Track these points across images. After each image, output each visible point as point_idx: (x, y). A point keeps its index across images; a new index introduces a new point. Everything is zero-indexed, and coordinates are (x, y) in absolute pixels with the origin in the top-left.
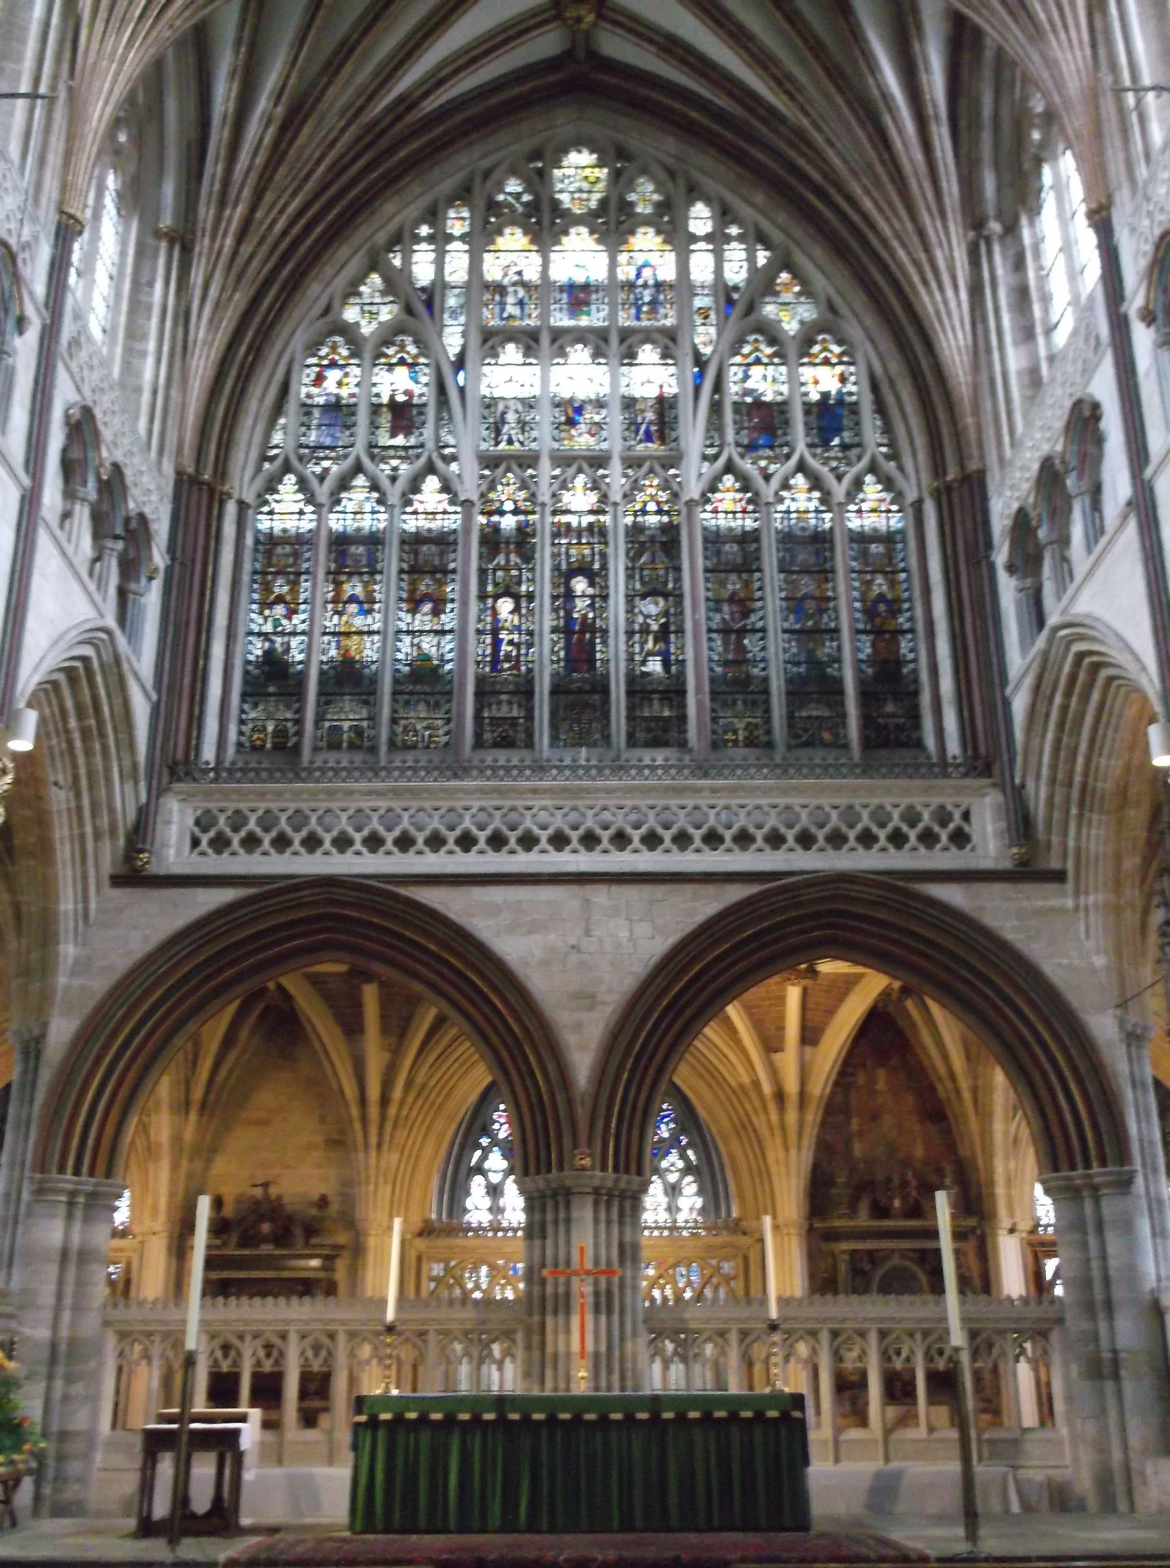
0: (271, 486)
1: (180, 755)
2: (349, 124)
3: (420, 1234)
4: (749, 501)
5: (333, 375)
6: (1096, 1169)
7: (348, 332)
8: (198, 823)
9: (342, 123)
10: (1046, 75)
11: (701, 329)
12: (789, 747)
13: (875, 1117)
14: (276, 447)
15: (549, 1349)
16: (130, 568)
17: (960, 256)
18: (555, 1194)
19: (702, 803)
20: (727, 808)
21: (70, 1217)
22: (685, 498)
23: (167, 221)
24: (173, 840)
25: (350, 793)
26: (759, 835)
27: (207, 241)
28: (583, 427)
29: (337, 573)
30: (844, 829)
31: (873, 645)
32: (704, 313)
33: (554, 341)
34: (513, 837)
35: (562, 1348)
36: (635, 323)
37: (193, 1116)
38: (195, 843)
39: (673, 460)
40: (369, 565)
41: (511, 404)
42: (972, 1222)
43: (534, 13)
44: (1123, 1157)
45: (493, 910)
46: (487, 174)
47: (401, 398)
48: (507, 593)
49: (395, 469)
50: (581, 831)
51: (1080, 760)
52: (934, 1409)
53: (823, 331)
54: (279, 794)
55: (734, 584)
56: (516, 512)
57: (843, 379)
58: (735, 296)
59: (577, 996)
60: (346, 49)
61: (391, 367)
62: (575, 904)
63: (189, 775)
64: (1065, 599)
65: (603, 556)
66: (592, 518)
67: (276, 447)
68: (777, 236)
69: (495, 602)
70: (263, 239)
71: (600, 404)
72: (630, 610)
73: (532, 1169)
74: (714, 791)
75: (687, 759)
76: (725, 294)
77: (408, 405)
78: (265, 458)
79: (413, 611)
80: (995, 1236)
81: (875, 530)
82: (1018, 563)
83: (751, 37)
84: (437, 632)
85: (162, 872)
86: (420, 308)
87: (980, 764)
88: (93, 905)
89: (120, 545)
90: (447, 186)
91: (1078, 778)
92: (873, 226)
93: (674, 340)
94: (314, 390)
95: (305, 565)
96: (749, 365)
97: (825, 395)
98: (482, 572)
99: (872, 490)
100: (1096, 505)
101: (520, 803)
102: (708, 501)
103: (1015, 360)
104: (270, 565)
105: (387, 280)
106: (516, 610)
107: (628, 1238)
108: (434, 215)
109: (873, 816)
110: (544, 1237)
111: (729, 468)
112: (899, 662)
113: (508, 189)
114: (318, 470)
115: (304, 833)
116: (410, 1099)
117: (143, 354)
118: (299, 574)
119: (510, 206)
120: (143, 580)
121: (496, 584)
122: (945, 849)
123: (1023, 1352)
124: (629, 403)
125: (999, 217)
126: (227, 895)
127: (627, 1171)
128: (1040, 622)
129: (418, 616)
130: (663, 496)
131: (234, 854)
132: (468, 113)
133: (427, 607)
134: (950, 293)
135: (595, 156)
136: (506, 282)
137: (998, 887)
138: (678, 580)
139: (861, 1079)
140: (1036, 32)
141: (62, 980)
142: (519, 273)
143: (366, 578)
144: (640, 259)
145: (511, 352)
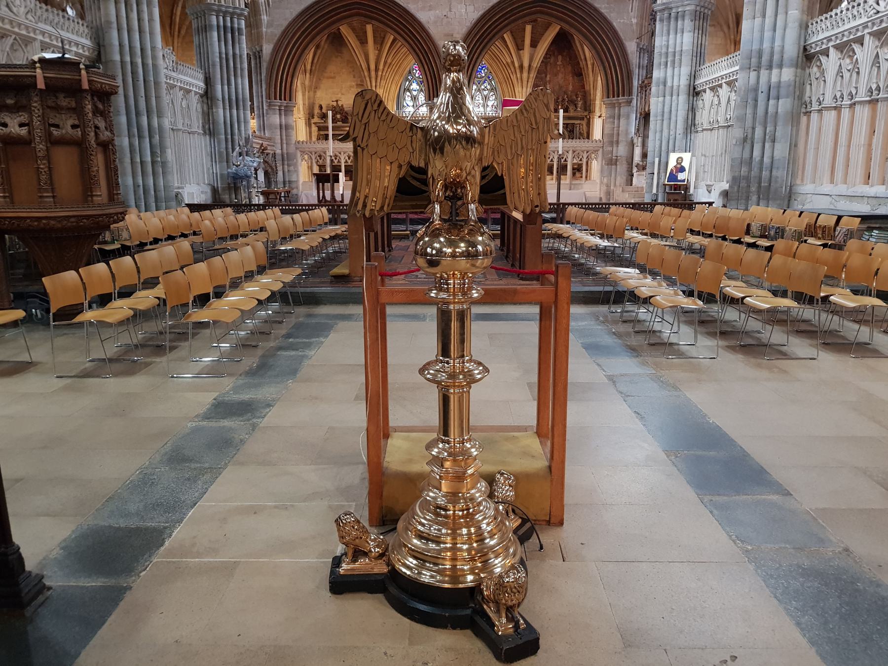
80: (593, 118)
116: (386, 69)
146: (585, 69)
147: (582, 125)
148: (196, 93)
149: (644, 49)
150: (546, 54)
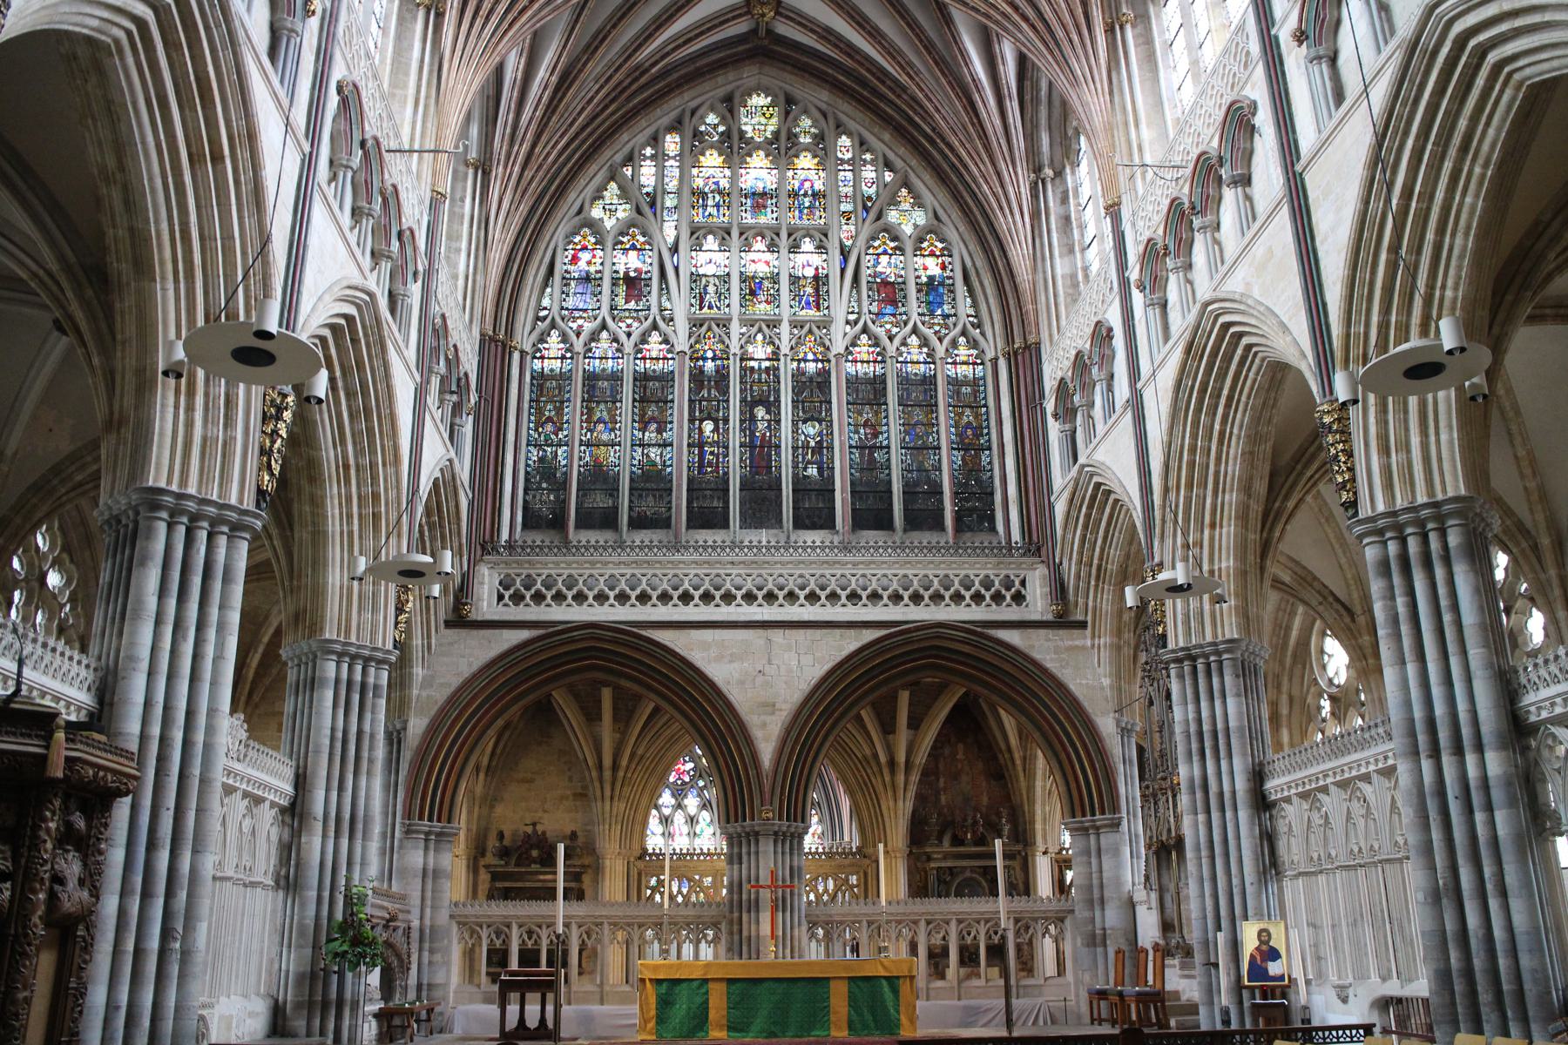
0: (542, 340)
1: (487, 537)
2: (602, 87)
3: (640, 858)
4: (878, 354)
5: (585, 256)
6: (1098, 817)
7: (594, 226)
8: (500, 584)
9: (597, 87)
10: (1080, 109)
11: (845, 227)
12: (905, 531)
13: (956, 777)
14: (545, 308)
15: (745, 933)
16: (457, 409)
17: (1025, 191)
18: (748, 834)
19: (847, 572)
20: (864, 576)
21: (426, 849)
22: (834, 351)
23: (473, 155)
24: (486, 596)
25: (607, 563)
26: (885, 595)
27: (501, 169)
28: (762, 298)
29: (589, 401)
30: (942, 591)
31: (963, 459)
32: (846, 215)
33: (741, 234)
34: (718, 595)
35: (753, 933)
36: (798, 222)
37: (482, 776)
38: (500, 597)
39: (825, 324)
40: (611, 396)
41: (711, 280)
42: (1019, 847)
43: (733, 9)
44: (1115, 808)
45: (705, 646)
46: (693, 113)
47: (632, 274)
48: (709, 418)
49: (629, 326)
50: (765, 591)
51: (1098, 549)
52: (989, 969)
53: (931, 232)
54: (557, 564)
55: (868, 414)
56: (713, 359)
57: (944, 267)
58: (869, 204)
59: (765, 705)
60: (601, 37)
61: (625, 251)
62: (762, 642)
63: (495, 550)
64: (1092, 446)
65: (777, 392)
66: (767, 364)
67: (545, 308)
68: (899, 163)
69: (701, 423)
70: (540, 166)
71: (775, 279)
72: (795, 431)
73: (732, 819)
74: (855, 564)
75: (836, 540)
76: (865, 204)
77: (638, 278)
78: (538, 318)
79: (643, 430)
80: (1034, 856)
81: (965, 376)
82: (1060, 412)
83: (882, 35)
84: (659, 446)
85: (479, 618)
86: (646, 209)
87: (1033, 548)
88: (433, 641)
89: (455, 398)
90: (665, 121)
91: (1096, 562)
92: (966, 167)
93: (826, 235)
94: (571, 268)
95: (567, 396)
96: (878, 255)
97: (932, 279)
98: (690, 400)
99: (963, 352)
100: (1110, 388)
101: (722, 572)
102: (851, 353)
103: (1061, 267)
104: (542, 395)
105: (620, 188)
106: (716, 429)
107: (795, 863)
108: (655, 140)
109: (961, 583)
110: (741, 863)
111: (865, 330)
112: (980, 470)
113: (708, 121)
114: (574, 326)
115: (575, 591)
117: (459, 250)
118: (562, 402)
119: (709, 134)
120: (464, 415)
121: (701, 411)
122: (1008, 605)
123: (1047, 930)
124: (795, 280)
125: (1052, 165)
126: (525, 635)
127: (795, 821)
128: (1075, 459)
129: (647, 434)
130: (821, 349)
131: (527, 605)
132: (682, 72)
133: (654, 426)
134: (1018, 217)
135: (769, 99)
136: (706, 190)
137: (1042, 632)
138: (829, 410)
139: (947, 751)
140: (1075, 82)
141: (415, 692)
142: (717, 183)
143: (610, 405)
144: (802, 175)
145: (711, 242)
146: (1009, 764)
147: (1014, 869)
148: (273, 805)
149: (1128, 731)
150: (935, 741)
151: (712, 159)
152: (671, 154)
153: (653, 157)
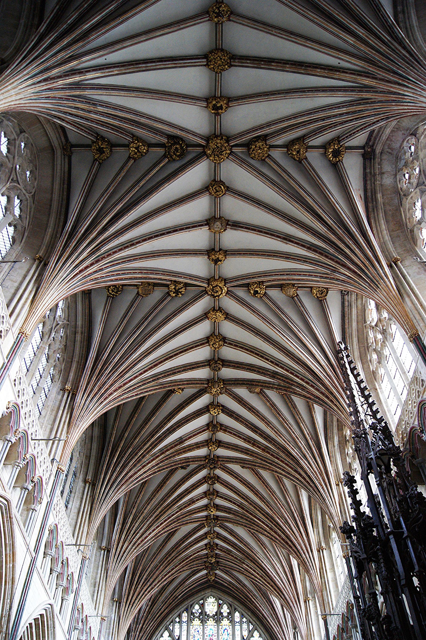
46: (191, 606)
90: (183, 609)
108: (180, 616)
136: (195, 634)
144: (224, 627)
151: (197, 622)
152: (185, 621)
153: (179, 622)
